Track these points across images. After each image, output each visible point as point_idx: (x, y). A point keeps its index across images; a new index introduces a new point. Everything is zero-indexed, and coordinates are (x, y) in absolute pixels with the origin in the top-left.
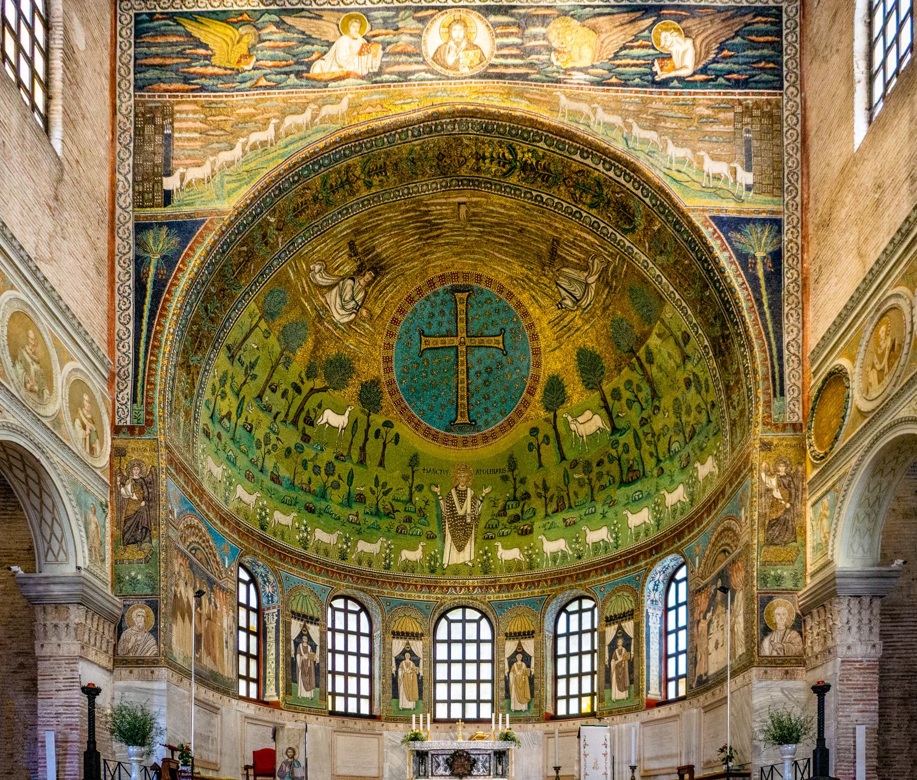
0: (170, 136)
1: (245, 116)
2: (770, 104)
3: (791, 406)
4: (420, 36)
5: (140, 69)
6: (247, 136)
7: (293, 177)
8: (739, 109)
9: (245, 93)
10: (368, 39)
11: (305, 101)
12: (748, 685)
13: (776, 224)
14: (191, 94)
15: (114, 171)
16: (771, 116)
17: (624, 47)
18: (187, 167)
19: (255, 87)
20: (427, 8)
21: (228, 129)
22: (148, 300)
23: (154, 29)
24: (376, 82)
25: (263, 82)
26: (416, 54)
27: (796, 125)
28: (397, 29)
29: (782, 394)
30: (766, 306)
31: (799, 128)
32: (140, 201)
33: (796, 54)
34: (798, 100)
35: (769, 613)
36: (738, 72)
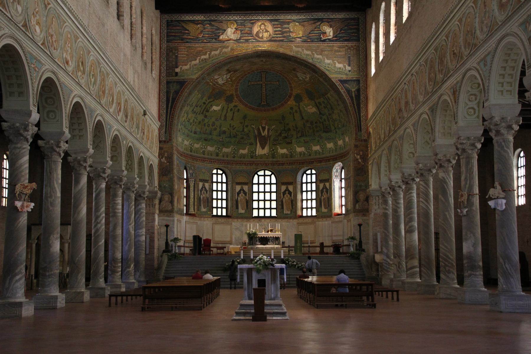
4: (251, 28)
6: (200, 56)
8: (346, 48)
15: (160, 66)
16: (356, 49)
18: (182, 65)
19: (202, 42)
20: (254, 20)
25: (205, 41)
28: (245, 26)
29: (361, 130)
30: (355, 105)
31: (365, 53)
34: (365, 45)
36: (346, 37)
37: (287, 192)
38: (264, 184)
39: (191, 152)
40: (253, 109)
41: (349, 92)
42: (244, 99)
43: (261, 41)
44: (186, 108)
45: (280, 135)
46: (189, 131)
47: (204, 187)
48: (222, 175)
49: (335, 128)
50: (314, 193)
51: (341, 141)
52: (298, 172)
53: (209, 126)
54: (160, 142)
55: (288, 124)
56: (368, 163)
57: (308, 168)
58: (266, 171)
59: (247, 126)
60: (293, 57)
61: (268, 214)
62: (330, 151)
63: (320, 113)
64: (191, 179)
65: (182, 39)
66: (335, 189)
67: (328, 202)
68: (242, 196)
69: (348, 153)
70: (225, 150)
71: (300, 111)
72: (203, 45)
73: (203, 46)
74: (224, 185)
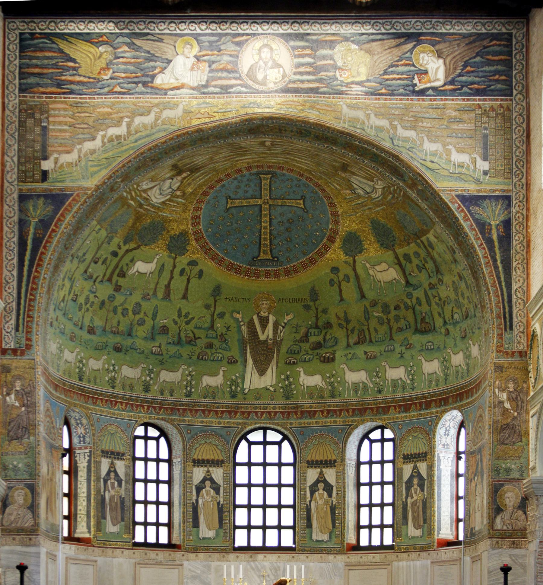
1: (103, 114)
2: (503, 107)
5: (23, 76)
6: (105, 130)
8: (479, 112)
9: (103, 96)
11: (149, 105)
14: (62, 96)
16: (503, 115)
19: (111, 92)
21: (90, 123)
23: (34, 45)
24: (204, 93)
26: (233, 71)
27: (522, 123)
31: (524, 125)
33: (522, 69)
34: (524, 104)
43: (261, 92)
44: (68, 266)
45: (305, 338)
50: (388, 489)
51: (461, 356)
53: (125, 312)
55: (325, 311)
57: (374, 424)
58: (268, 431)
59: (222, 315)
60: (342, 133)
61: (272, 541)
63: (407, 282)
65: (59, 85)
69: (477, 387)
72: (111, 99)
73: (113, 104)
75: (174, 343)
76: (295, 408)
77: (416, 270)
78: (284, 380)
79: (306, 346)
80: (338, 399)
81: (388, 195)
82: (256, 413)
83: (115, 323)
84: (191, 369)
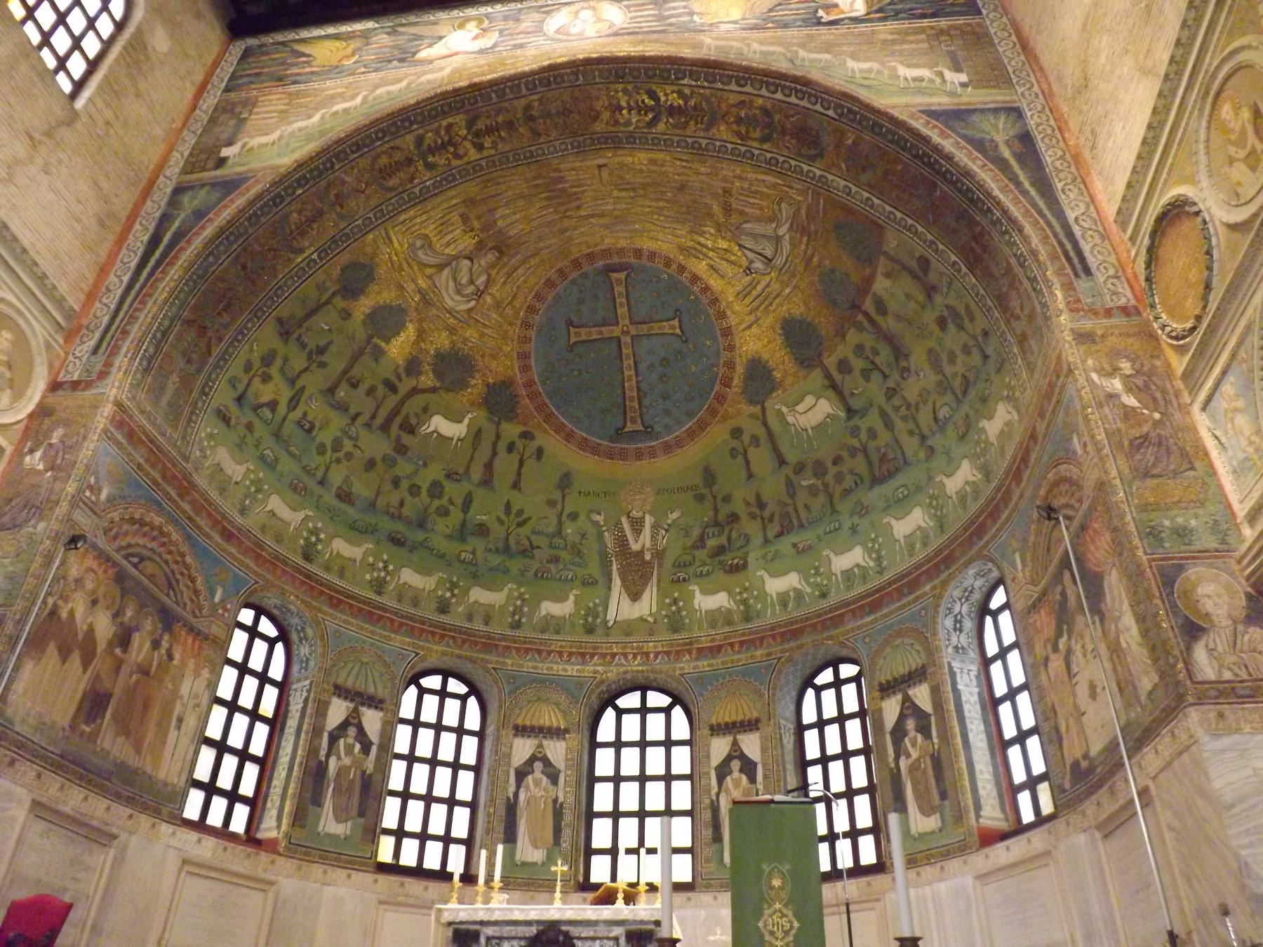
0: (245, 119)
3: (1109, 286)
7: (376, 133)
8: (933, 32)
10: (484, 30)
12: (1187, 748)
13: (1016, 113)
17: (780, 4)
18: (252, 137)
22: (158, 254)
25: (363, 70)
29: (1088, 271)
30: (1027, 185)
31: (1014, 38)
32: (191, 166)
34: (1005, 19)
35: (1187, 594)
37: (736, 765)
38: (643, 744)
39: (307, 557)
40: (595, 450)
41: (981, 146)
42: (558, 408)
45: (701, 542)
46: (304, 468)
47: (352, 722)
48: (463, 699)
49: (923, 438)
52: (780, 672)
54: (55, 386)
55: (727, 499)
56: (1185, 410)
59: (574, 516)
62: (911, 547)
63: (850, 412)
64: (299, 681)
66: (966, 707)
67: (939, 777)
68: (537, 783)
70: (479, 595)
71: (771, 435)
72: (351, 79)
74: (470, 744)
75: (497, 551)
76: (686, 644)
77: (861, 381)
78: (670, 605)
79: (702, 554)
80: (755, 624)
81: (801, 242)
82: (625, 655)
83: (395, 502)
84: (523, 590)
